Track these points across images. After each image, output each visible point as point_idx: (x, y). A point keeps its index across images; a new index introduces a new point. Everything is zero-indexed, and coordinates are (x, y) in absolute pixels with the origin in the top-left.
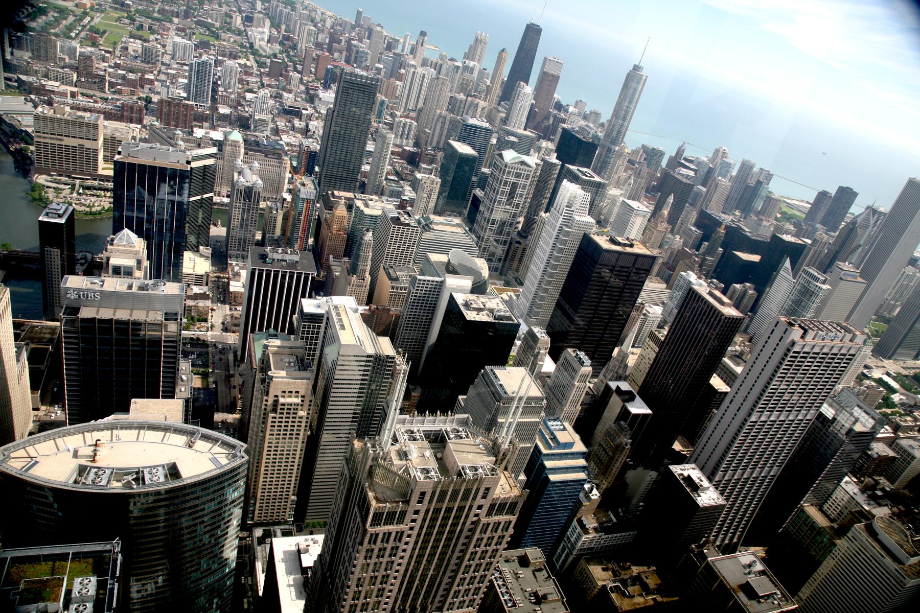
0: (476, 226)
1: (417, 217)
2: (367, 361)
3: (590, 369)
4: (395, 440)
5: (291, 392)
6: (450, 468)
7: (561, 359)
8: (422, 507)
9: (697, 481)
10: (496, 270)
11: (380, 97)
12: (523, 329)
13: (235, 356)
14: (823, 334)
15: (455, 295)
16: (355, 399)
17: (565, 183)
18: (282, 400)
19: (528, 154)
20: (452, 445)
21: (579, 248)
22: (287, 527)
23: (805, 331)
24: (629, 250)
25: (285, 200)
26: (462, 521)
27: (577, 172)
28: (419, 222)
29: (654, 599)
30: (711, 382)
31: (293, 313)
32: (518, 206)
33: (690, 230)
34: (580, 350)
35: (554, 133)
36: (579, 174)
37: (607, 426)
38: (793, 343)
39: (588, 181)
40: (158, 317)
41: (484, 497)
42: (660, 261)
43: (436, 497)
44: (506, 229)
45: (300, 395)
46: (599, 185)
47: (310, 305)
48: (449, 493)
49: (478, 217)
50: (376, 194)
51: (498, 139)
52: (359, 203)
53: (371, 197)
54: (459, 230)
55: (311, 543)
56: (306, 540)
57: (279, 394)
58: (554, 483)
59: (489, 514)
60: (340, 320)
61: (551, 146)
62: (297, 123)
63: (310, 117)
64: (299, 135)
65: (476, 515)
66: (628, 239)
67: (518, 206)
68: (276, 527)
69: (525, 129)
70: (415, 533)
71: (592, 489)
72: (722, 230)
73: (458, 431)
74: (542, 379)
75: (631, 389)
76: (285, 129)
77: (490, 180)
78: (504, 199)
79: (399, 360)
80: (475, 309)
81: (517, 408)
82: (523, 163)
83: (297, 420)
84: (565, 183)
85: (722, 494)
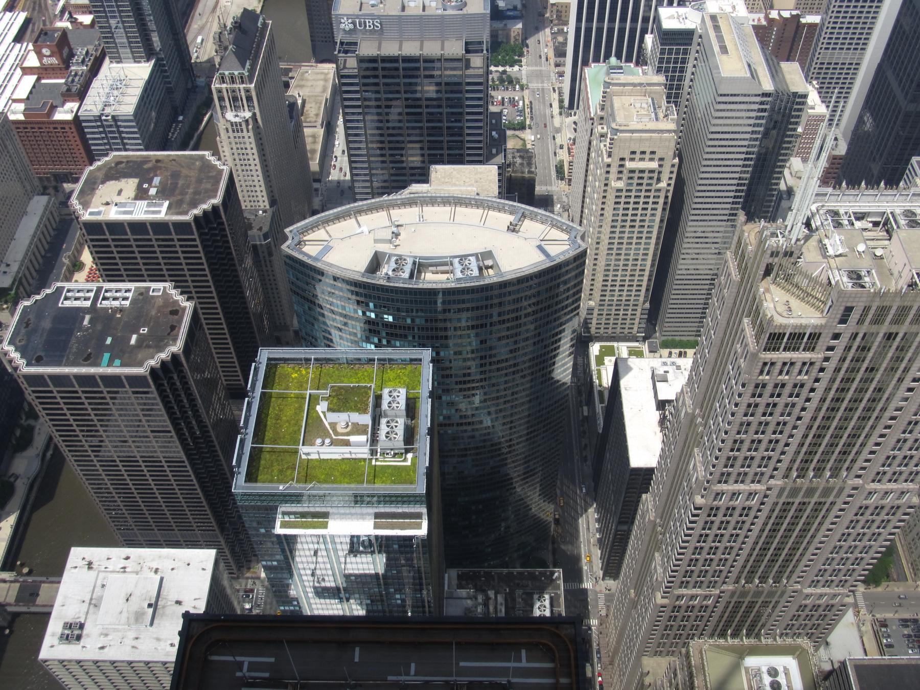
2: (762, 103)
4: (808, 224)
5: (643, 153)
8: (846, 330)
13: (561, 101)
20: (903, 233)
22: (636, 344)
26: (909, 355)
31: (644, 31)
40: (455, 48)
45: (657, 157)
48: (893, 312)
55: (671, 369)
56: (665, 364)
57: (627, 155)
60: (720, 38)
68: (621, 344)
70: (831, 366)
79: (814, 98)
83: (652, 194)
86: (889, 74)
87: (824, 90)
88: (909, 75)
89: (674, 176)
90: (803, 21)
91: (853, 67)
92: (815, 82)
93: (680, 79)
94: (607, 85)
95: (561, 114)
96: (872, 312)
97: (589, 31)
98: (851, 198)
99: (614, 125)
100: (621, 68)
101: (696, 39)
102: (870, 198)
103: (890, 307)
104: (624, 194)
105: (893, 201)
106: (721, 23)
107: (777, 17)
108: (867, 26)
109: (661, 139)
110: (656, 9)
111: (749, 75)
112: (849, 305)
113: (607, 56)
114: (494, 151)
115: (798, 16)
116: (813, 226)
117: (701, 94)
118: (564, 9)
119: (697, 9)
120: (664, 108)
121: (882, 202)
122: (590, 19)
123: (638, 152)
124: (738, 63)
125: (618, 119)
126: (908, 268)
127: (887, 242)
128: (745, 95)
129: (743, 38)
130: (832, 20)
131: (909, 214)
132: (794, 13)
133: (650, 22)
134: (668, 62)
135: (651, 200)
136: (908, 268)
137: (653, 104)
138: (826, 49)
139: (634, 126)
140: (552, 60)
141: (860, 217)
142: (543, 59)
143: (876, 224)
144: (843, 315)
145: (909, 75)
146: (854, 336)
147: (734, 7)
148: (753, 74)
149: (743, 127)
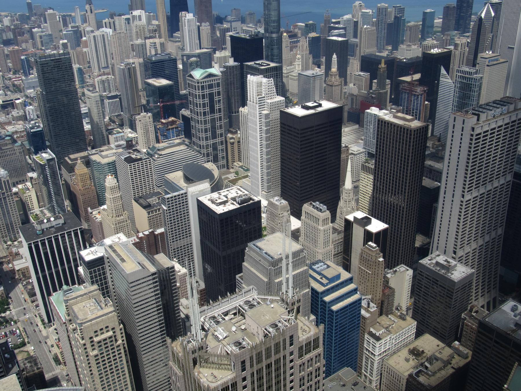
0: (194, 139)
1: (145, 150)
2: (154, 279)
3: (328, 212)
4: (203, 329)
5: (102, 329)
6: (256, 334)
7: (303, 213)
9: (445, 263)
10: (223, 166)
11: (75, 67)
12: (264, 203)
13: (43, 321)
14: (493, 112)
15: (200, 199)
16: (156, 313)
17: (250, 78)
18: (96, 339)
19: (211, 67)
20: (249, 313)
21: (281, 123)
23: (478, 116)
24: (320, 109)
25: (31, 178)
26: (282, 370)
27: (255, 65)
28: (148, 154)
29: (452, 367)
30: (423, 184)
31: (76, 266)
32: (220, 109)
33: (359, 75)
34: (314, 202)
35: (224, 43)
36: (257, 66)
37: (359, 251)
38: (473, 129)
39: (266, 69)
41: (291, 344)
42: (346, 109)
43: (255, 361)
44: (219, 132)
45: (110, 328)
46: (275, 68)
47: (88, 254)
49: (193, 131)
50: (104, 144)
51: (184, 64)
52: (94, 158)
53: (102, 149)
54: (183, 147)
57: (93, 335)
58: (337, 312)
59: (301, 356)
60: (119, 256)
61: (227, 53)
62: (15, 113)
63: (25, 104)
64: (21, 122)
65: (291, 361)
66: (315, 102)
67: (220, 109)
69: (200, 49)
71: (369, 304)
72: (383, 65)
73: (249, 302)
74: (295, 235)
75: (365, 215)
76: (7, 121)
77: (190, 98)
78: (207, 109)
79: (178, 267)
80: (221, 204)
81: (288, 264)
82: (211, 75)
83: (116, 350)
84: (250, 78)
85: (466, 264)
86: (207, 242)
87: (181, 261)
88: (216, 240)
89: (124, 334)
90: (156, 233)
91: (189, 245)
92: (175, 259)
93: (106, 283)
94: (66, 301)
95: (45, 328)
96: (254, 358)
97: (45, 277)
98: (217, 307)
99: (79, 322)
100: (71, 289)
101: (106, 261)
102: (226, 303)
103: (262, 351)
104: (100, 356)
105: (237, 300)
106: (116, 248)
107: (143, 236)
108: (187, 225)
109: (108, 318)
110: (79, 253)
111: (141, 268)
112: (242, 360)
113: (61, 286)
114: (10, 366)
115: (153, 232)
116: (206, 328)
117: (120, 287)
118: (26, 271)
119: (101, 245)
120: (103, 301)
121: (233, 302)
122: (43, 270)
123: (98, 330)
124: (132, 264)
125: (80, 317)
126: (259, 328)
127: (244, 321)
128: (143, 278)
129: (130, 251)
130: (170, 228)
131: (247, 302)
132: (150, 231)
133: (78, 260)
134: (96, 277)
135: (116, 353)
136: (259, 328)
137: (96, 301)
138: (173, 242)
139: (90, 317)
140: (29, 300)
141: (226, 314)
142: (23, 301)
143: (235, 314)
144: (242, 367)
145: (216, 240)
146: (252, 375)
147: (119, 238)
148: (143, 267)
149: (149, 293)
